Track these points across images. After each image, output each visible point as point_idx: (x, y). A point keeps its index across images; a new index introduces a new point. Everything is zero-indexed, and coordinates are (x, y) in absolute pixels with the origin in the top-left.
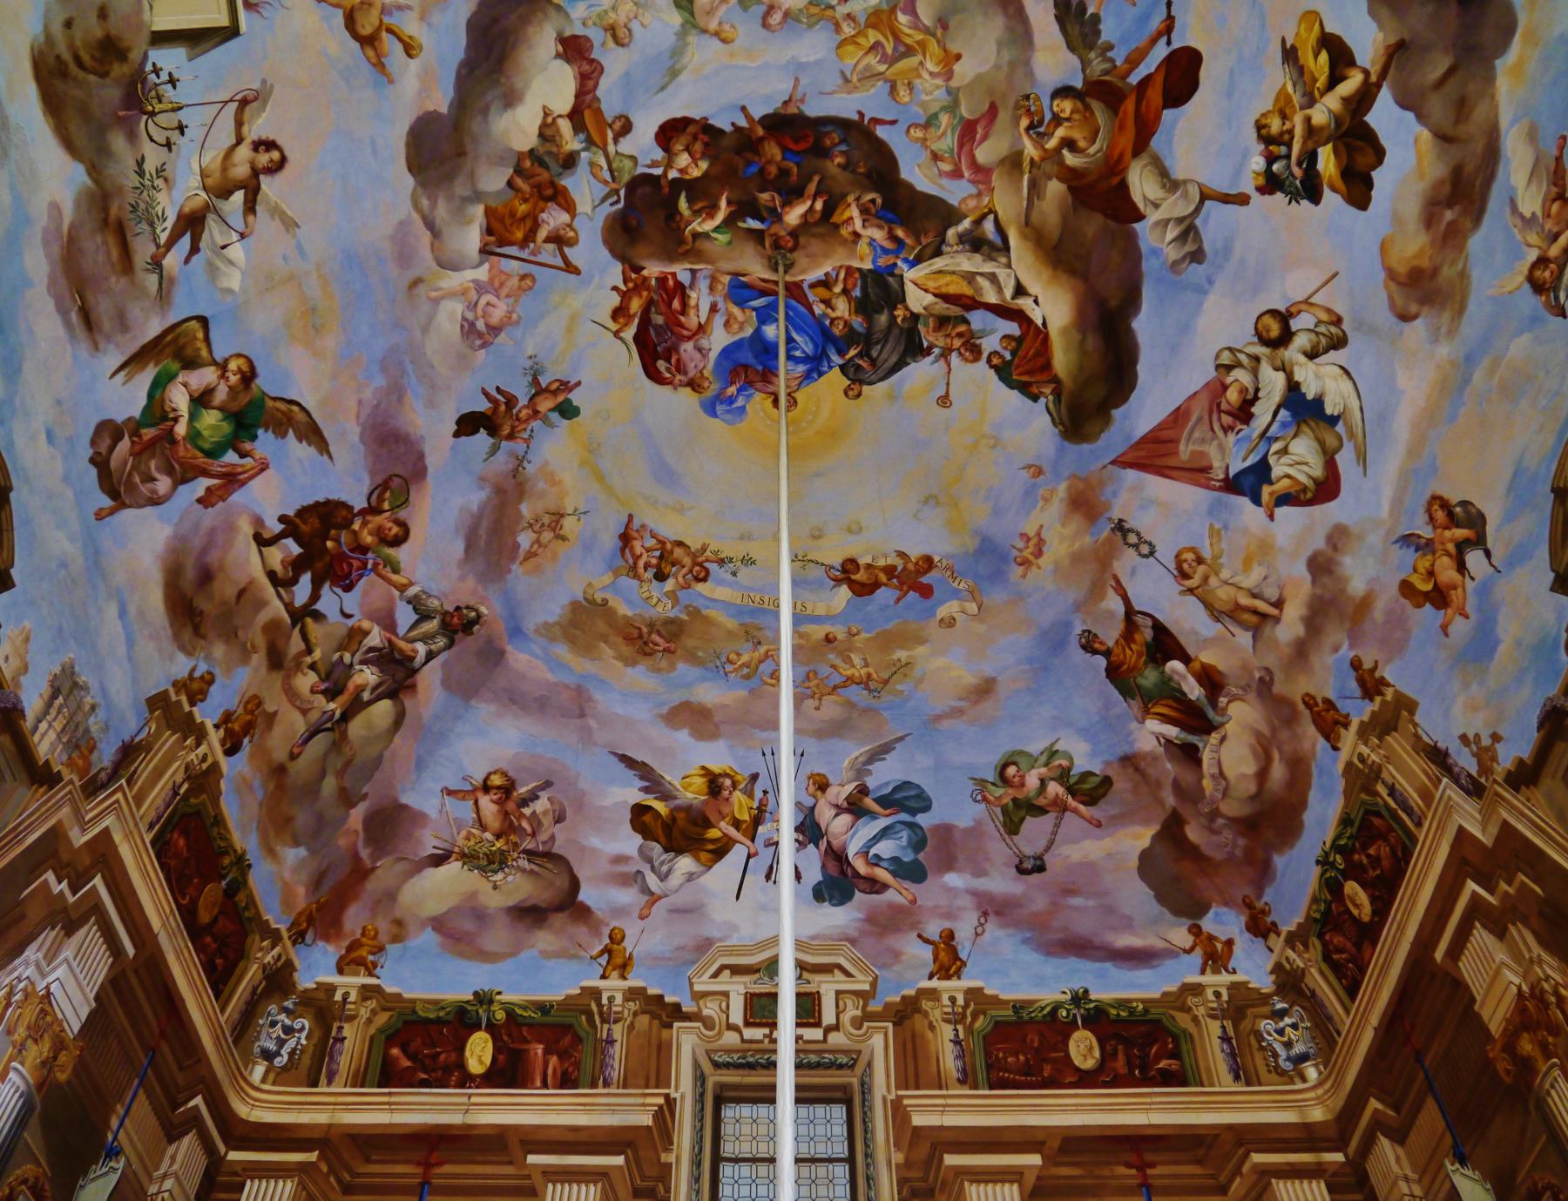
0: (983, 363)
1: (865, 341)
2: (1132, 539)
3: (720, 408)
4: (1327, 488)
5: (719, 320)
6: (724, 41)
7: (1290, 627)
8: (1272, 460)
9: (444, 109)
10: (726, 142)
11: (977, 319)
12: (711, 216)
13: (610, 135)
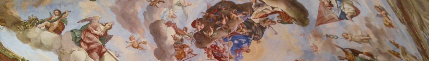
0: (277, 24)
1: (254, 33)
2: (331, 37)
3: (238, 59)
4: (357, 12)
5: (226, 46)
6: (190, 5)
7: (374, 39)
8: (343, 11)
9: (157, 47)
10: (204, 19)
11: (270, 17)
12: (211, 32)
13: (185, 32)
